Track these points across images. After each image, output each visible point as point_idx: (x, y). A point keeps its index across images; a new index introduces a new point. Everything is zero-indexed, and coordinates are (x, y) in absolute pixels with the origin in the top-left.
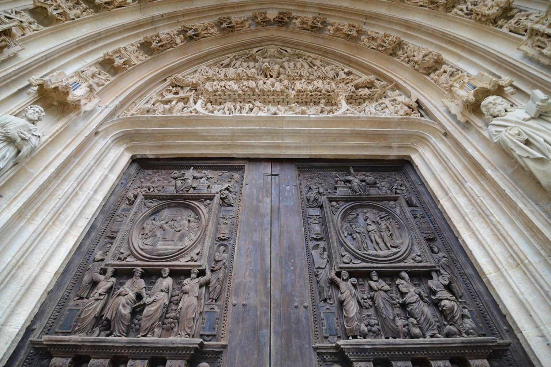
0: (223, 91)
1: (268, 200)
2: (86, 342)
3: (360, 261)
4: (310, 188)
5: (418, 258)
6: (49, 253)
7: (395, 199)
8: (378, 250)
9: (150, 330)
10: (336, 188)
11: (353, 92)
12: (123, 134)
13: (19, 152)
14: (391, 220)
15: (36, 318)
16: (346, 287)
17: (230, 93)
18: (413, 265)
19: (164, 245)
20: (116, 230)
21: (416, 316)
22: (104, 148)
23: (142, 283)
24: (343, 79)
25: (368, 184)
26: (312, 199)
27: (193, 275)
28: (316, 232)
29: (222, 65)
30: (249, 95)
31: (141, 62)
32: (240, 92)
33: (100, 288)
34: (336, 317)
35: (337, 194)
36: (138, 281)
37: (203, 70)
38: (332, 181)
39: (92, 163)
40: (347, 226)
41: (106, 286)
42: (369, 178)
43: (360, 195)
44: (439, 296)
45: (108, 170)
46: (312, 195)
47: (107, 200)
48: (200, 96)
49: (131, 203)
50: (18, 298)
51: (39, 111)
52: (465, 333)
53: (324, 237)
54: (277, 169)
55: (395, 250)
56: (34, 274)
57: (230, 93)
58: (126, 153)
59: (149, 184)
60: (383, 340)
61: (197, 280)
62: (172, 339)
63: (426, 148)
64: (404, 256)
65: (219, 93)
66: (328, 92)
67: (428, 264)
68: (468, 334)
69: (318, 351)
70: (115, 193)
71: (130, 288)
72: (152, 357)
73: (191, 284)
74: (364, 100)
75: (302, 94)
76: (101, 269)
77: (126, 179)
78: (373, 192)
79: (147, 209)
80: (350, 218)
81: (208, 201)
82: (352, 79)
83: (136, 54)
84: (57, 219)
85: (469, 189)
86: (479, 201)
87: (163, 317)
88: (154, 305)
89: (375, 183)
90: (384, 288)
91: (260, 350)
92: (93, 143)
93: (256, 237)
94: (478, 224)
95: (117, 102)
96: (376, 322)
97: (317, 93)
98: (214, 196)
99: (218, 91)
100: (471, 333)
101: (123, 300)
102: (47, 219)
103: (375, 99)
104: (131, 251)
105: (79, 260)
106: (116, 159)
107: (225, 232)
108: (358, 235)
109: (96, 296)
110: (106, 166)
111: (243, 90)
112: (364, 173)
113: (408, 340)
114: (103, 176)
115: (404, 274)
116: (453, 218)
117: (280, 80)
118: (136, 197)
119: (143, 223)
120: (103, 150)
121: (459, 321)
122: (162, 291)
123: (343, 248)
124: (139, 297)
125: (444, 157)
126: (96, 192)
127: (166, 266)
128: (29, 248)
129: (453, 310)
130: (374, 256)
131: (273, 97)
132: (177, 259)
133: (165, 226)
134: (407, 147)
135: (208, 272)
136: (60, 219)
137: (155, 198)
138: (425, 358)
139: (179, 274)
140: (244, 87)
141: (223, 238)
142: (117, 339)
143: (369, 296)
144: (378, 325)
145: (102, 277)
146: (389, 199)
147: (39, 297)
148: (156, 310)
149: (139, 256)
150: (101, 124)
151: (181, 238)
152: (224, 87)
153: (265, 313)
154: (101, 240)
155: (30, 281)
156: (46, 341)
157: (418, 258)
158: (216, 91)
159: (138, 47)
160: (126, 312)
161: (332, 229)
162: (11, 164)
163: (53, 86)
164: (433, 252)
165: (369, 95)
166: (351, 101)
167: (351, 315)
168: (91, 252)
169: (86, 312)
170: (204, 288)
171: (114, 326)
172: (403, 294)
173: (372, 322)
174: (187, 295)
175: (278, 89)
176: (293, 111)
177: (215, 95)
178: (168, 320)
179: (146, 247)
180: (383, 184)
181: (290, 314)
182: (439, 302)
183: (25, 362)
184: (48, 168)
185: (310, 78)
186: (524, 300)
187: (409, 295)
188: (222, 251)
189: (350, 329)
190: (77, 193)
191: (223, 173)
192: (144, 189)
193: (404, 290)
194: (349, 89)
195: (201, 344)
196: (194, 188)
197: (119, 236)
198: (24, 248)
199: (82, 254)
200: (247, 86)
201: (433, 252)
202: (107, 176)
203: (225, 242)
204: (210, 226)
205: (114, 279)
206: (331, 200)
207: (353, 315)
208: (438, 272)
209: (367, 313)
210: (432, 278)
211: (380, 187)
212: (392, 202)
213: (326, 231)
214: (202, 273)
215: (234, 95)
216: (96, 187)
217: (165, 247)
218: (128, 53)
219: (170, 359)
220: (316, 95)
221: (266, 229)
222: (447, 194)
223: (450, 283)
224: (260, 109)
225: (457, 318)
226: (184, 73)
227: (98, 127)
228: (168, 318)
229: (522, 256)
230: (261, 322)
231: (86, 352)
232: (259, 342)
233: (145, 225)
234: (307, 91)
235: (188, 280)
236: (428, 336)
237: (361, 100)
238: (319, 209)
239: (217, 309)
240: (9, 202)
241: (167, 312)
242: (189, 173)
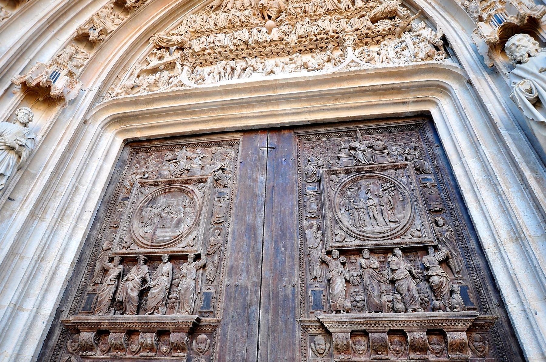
0: (212, 48)
1: (262, 178)
2: (104, 320)
3: (354, 239)
4: (309, 161)
5: (419, 233)
6: (63, 247)
7: (404, 167)
8: (375, 226)
9: (155, 309)
10: (338, 158)
11: (369, 29)
12: (111, 118)
13: (20, 157)
14: (395, 192)
15: (63, 301)
16: (336, 266)
17: (220, 49)
18: (408, 241)
19: (162, 232)
20: (118, 220)
21: (402, 293)
22: (95, 138)
23: (145, 269)
24: (360, 8)
25: (375, 150)
26: (310, 174)
27: (189, 260)
28: (312, 211)
29: (211, 8)
30: (242, 49)
31: (118, 26)
32: (232, 47)
33: (111, 275)
34: (323, 294)
35: (339, 165)
36: (142, 267)
37: (189, 20)
38: (335, 150)
39: (86, 156)
40: (345, 203)
41: (115, 273)
42: (378, 142)
43: (363, 165)
44: (430, 272)
45: (102, 161)
46: (311, 168)
47: (106, 191)
48: (185, 62)
49: (129, 191)
50: (45, 287)
51: (28, 113)
52: (450, 308)
53: (320, 215)
54: (274, 139)
55: (393, 225)
56: (54, 266)
57: (220, 49)
58: (117, 139)
59: (143, 170)
60: (367, 315)
61: (194, 264)
62: (173, 315)
63: (448, 100)
64: (402, 231)
65: (208, 51)
66: (337, 33)
67: (426, 240)
68: (452, 308)
69: (302, 324)
70: (112, 183)
71: (137, 273)
72: (158, 330)
73: (189, 268)
75: (304, 39)
76: (110, 258)
77: (121, 166)
78: (382, 160)
79: (144, 197)
80: (349, 192)
81: (202, 185)
82: (371, 7)
83: (111, 18)
84: (64, 215)
85: (483, 154)
86: (489, 167)
87: (167, 299)
88: (157, 289)
89: (385, 148)
90: (372, 266)
91: (249, 325)
92: (83, 133)
93: (249, 219)
94: (486, 194)
95: (99, 83)
96: (363, 298)
97: (322, 36)
98: (207, 178)
99: (206, 49)
100: (456, 308)
101: (130, 284)
102: (56, 217)
104: (134, 240)
105: (89, 251)
106: (108, 147)
107: (219, 216)
108: (355, 211)
109: (108, 282)
110: (100, 156)
111: (235, 45)
112: (374, 136)
113: (393, 314)
114: (99, 167)
115: (398, 251)
116: (464, 187)
117: (281, 20)
118: (132, 185)
119: (142, 212)
120: (94, 140)
121: (445, 296)
122: (163, 275)
123: (337, 226)
124: (144, 281)
125: (462, 112)
126: (94, 184)
127: (165, 253)
128: (46, 243)
129: (442, 285)
130: (369, 233)
131: (271, 48)
132: (175, 245)
133: (163, 214)
134: (425, 101)
135: (203, 256)
136: (66, 214)
137: (151, 185)
138: (403, 330)
139: (177, 259)
140: (235, 41)
141: (218, 222)
142: (130, 317)
143: (359, 274)
144: (364, 301)
145: (111, 265)
146: (396, 168)
147: (61, 285)
148: (159, 292)
149: (141, 244)
150: (88, 111)
151: (178, 224)
152: (213, 43)
153: (256, 291)
154: (106, 230)
155: (52, 272)
156: (73, 320)
157: (419, 233)
158: (204, 50)
159: (112, 8)
160: (135, 294)
161: (327, 206)
162: (16, 170)
163: (34, 83)
164: (437, 225)
165: (390, 29)
166: (367, 40)
167: (335, 293)
168: (98, 243)
169: (102, 296)
170: (201, 271)
171: (126, 307)
172: (393, 271)
173: (358, 298)
174: (185, 278)
175: (276, 38)
176: (295, 63)
177: (204, 54)
178: (170, 301)
179: (147, 235)
180: (394, 148)
181: (279, 292)
182: (429, 278)
183: (60, 337)
184: (48, 167)
185: (318, 13)
186: (513, 276)
187: (399, 271)
188: (217, 235)
189: (334, 305)
190: (77, 188)
191: (218, 150)
192: (139, 176)
193: (394, 267)
194: (363, 25)
195: (198, 320)
196: (188, 170)
197: (122, 225)
198: (42, 245)
199: (91, 244)
200: (239, 38)
201: (437, 225)
202: (102, 166)
203: (219, 226)
204: (203, 211)
205: (121, 266)
206: (330, 173)
207: (338, 291)
208: (436, 248)
209: (355, 290)
210: (428, 254)
211: (391, 152)
212: (400, 171)
213: (321, 209)
214: (198, 257)
215: (226, 51)
216: (93, 180)
217: (164, 234)
218: (102, 20)
219: (173, 332)
220: (322, 39)
221: (260, 210)
222: (461, 159)
223: (447, 258)
224: (254, 68)
225: (444, 293)
226: (168, 29)
227: (85, 116)
228: (170, 299)
229: (519, 230)
230: (251, 301)
231: (105, 328)
232: (249, 317)
233: (143, 213)
235: (186, 264)
236: (410, 310)
237: (379, 38)
238: (318, 183)
239: (213, 290)
240: (21, 205)
241: (169, 293)
242: (182, 154)
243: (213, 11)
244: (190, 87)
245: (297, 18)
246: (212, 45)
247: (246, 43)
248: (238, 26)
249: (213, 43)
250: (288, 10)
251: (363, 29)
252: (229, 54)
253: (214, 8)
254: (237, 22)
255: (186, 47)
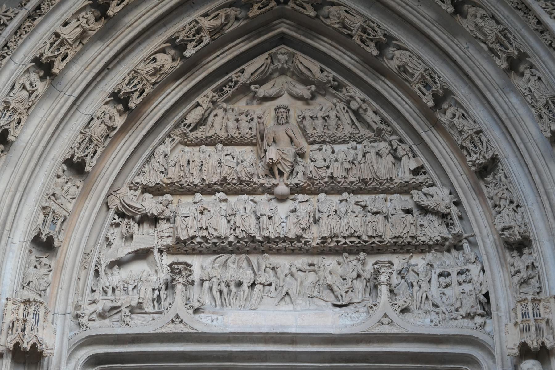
0: (203, 237)
11: (413, 237)
24: (406, 182)
30: (246, 242)
65: (199, 240)
74: (430, 247)
82: (421, 183)
97: (353, 239)
103: (445, 247)
152: (207, 229)
200: (242, 228)
220: (352, 242)
234: (337, 237)
243: (191, 131)
244: (192, 328)
245: (319, 183)
246: (205, 233)
247: (253, 239)
248: (235, 184)
249: (207, 229)
250: (309, 172)
251: (404, 237)
252: (228, 246)
253: (193, 125)
254: (233, 179)
255: (162, 217)
